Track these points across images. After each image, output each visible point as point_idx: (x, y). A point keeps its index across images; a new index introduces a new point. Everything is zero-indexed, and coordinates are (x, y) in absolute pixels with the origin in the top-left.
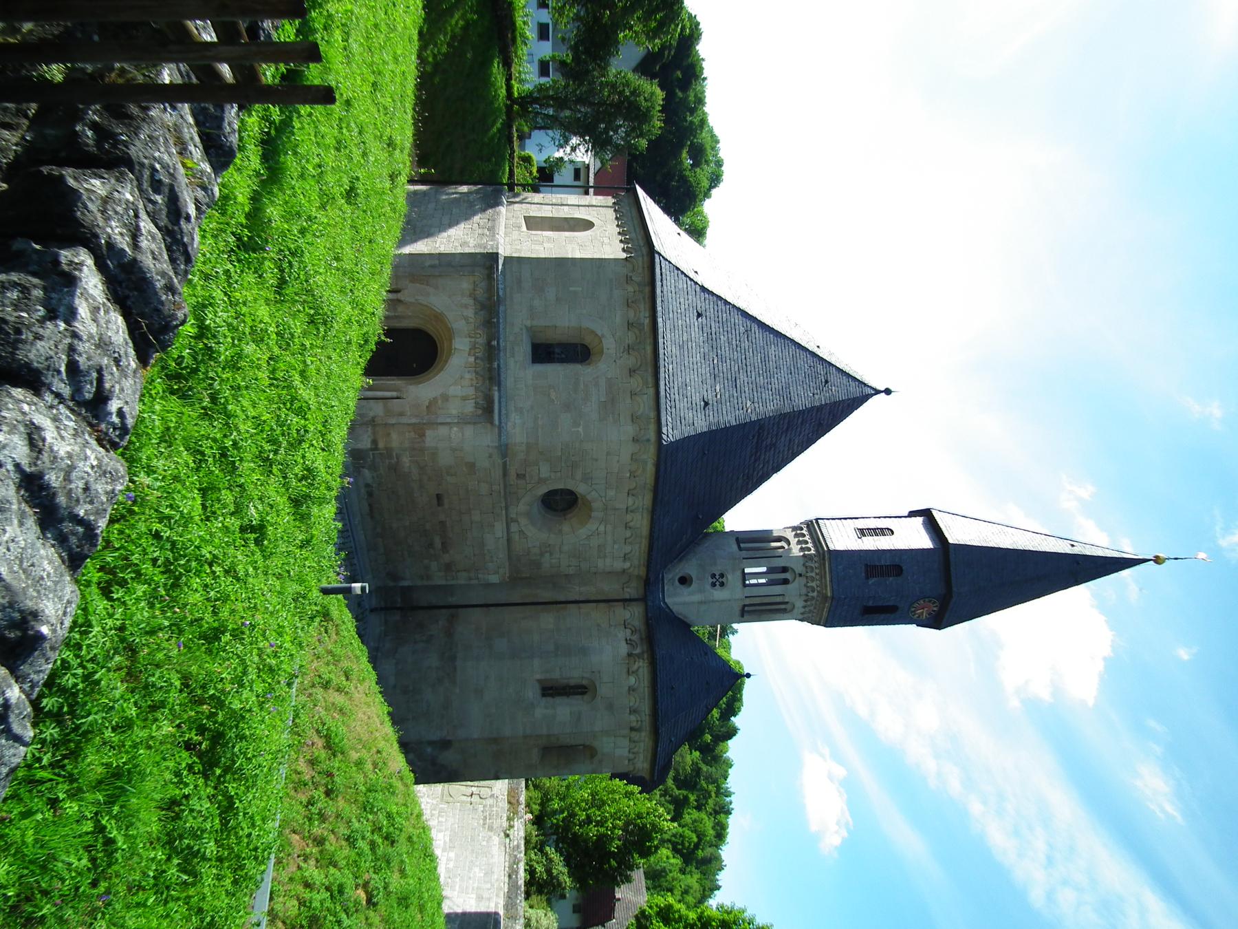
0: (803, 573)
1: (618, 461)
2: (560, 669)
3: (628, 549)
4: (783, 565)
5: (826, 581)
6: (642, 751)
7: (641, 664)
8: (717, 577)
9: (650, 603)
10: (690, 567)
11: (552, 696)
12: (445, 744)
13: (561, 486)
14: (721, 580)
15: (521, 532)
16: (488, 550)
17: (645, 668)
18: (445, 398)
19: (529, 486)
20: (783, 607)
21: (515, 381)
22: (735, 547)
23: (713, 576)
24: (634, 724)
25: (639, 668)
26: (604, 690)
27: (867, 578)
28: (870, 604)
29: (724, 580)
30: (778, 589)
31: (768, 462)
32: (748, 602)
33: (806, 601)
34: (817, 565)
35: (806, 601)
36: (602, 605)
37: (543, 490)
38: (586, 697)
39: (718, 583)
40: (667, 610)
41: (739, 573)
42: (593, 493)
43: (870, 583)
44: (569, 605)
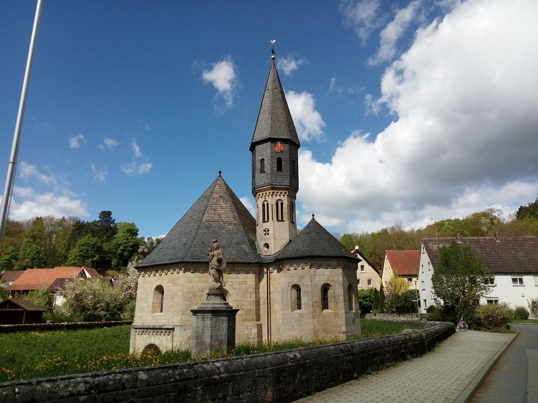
6: (325, 263)
8: (266, 233)
10: (260, 244)
11: (300, 305)
17: (287, 262)
23: (265, 234)
24: (308, 267)
26: (295, 282)
27: (264, 172)
29: (267, 230)
32: (275, 219)
33: (276, 195)
34: (261, 193)
39: (268, 232)
40: (278, 253)
43: (266, 171)
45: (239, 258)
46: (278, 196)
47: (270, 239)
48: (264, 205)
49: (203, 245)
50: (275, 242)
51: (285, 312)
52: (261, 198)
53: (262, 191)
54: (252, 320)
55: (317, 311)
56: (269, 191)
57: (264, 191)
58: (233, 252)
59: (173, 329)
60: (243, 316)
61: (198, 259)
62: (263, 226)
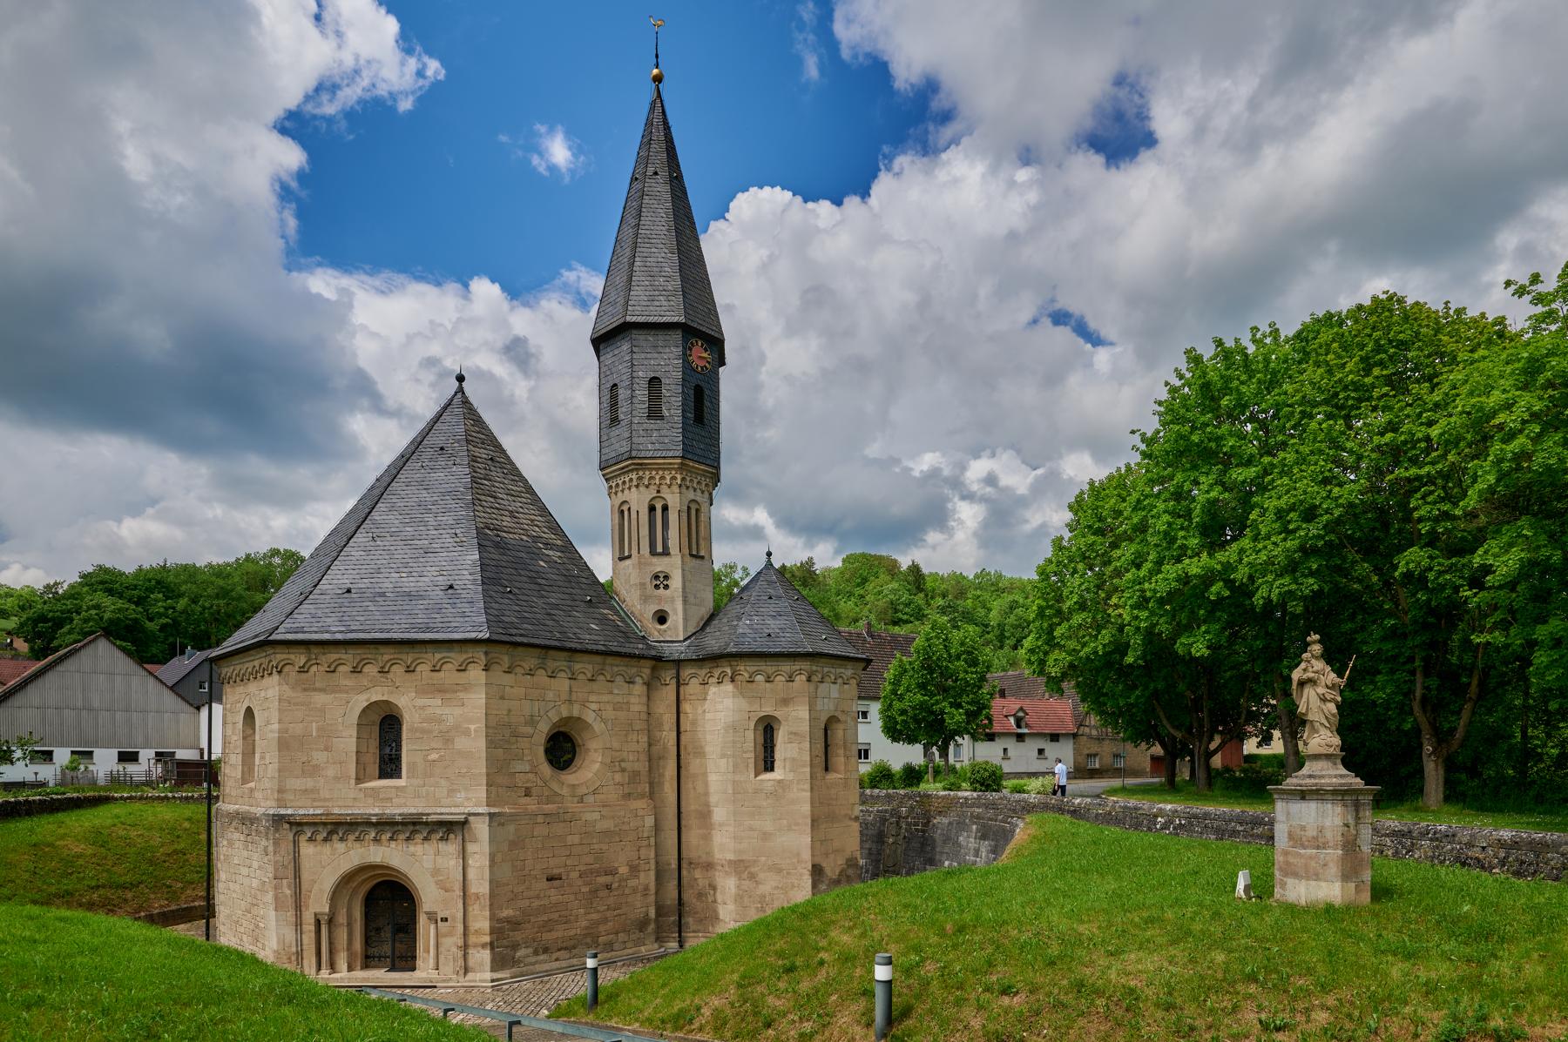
0: (655, 487)
1: (512, 687)
2: (745, 752)
3: (619, 679)
4: (646, 511)
5: (664, 464)
7: (742, 668)
8: (658, 583)
9: (682, 656)
12: (817, 871)
13: (541, 750)
14: (662, 579)
15: (594, 793)
16: (615, 826)
18: (436, 872)
19: (540, 783)
20: (693, 512)
21: (419, 797)
22: (628, 562)
23: (657, 587)
25: (746, 670)
26: (768, 710)
28: (691, 416)
29: (662, 575)
30: (673, 517)
31: (532, 521)
33: (688, 488)
34: (647, 473)
35: (688, 488)
36: (686, 707)
37: (546, 769)
38: (775, 727)
39: (665, 583)
41: (655, 560)
42: (550, 714)
44: (683, 743)
45: (615, 644)
46: (691, 490)
47: (673, 600)
48: (652, 509)
49: (511, 596)
50: (685, 611)
51: (737, 778)
52: (647, 487)
53: (651, 469)
54: (642, 796)
55: (818, 775)
56: (673, 472)
57: (657, 470)
58: (593, 626)
59: (465, 823)
60: (626, 786)
61: (521, 635)
62: (651, 564)
